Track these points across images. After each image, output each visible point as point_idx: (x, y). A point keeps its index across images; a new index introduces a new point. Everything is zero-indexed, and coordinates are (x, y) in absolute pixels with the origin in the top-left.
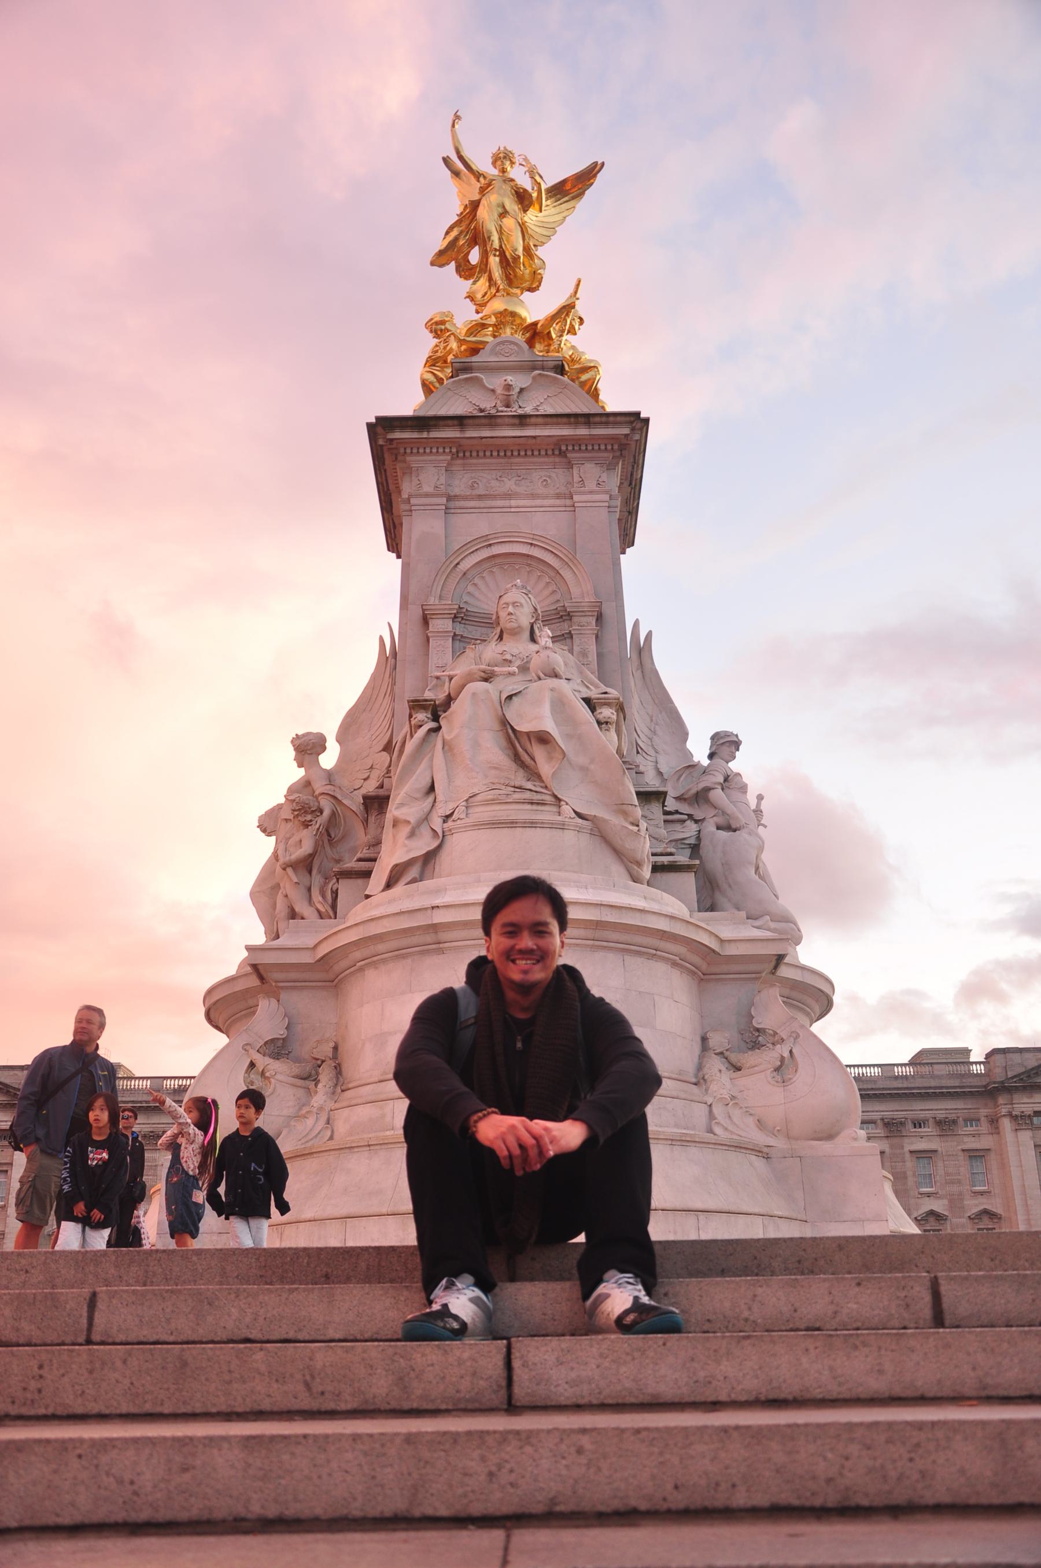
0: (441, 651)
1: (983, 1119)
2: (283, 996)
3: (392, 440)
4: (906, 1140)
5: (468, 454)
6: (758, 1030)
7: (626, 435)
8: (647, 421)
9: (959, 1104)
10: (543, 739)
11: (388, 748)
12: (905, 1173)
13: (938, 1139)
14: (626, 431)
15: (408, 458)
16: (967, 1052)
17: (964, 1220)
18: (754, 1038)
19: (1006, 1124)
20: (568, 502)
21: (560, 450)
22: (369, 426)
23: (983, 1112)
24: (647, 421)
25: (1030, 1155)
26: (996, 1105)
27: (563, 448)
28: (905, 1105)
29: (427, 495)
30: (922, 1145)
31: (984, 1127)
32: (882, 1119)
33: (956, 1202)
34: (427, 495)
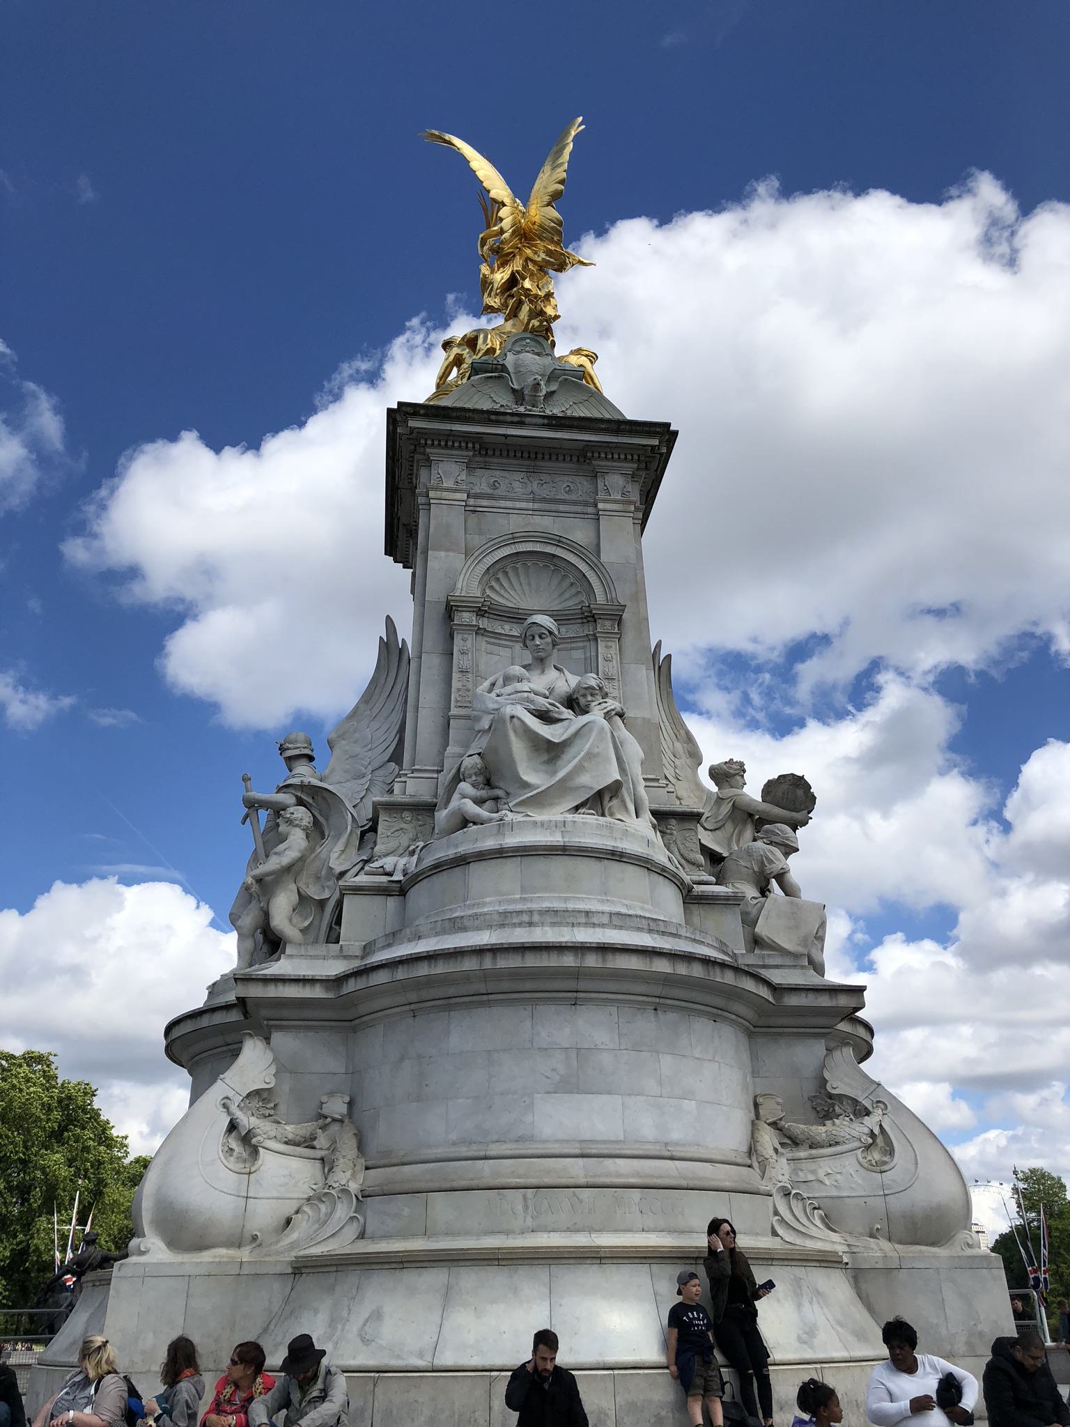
2: (277, 1037)
3: (412, 430)
5: (490, 452)
6: (831, 1096)
7: (653, 447)
8: (676, 433)
14: (656, 442)
15: (428, 450)
18: (826, 1104)
20: (591, 510)
21: (585, 456)
22: (390, 411)
24: (676, 433)
27: (589, 454)
29: (448, 490)
34: (448, 490)
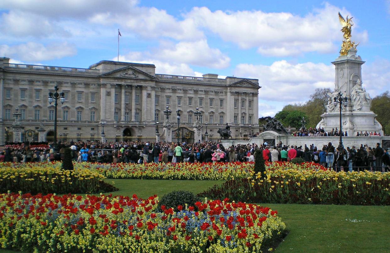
0: (351, 85)
1: (224, 92)
4: (208, 95)
9: (220, 88)
10: (368, 99)
11: (345, 92)
12: (207, 103)
13: (214, 96)
16: (217, 75)
17: (218, 114)
19: (229, 94)
23: (224, 90)
25: (233, 102)
26: (227, 89)
28: (209, 87)
30: (211, 97)
31: (224, 94)
32: (204, 90)
33: (217, 110)
